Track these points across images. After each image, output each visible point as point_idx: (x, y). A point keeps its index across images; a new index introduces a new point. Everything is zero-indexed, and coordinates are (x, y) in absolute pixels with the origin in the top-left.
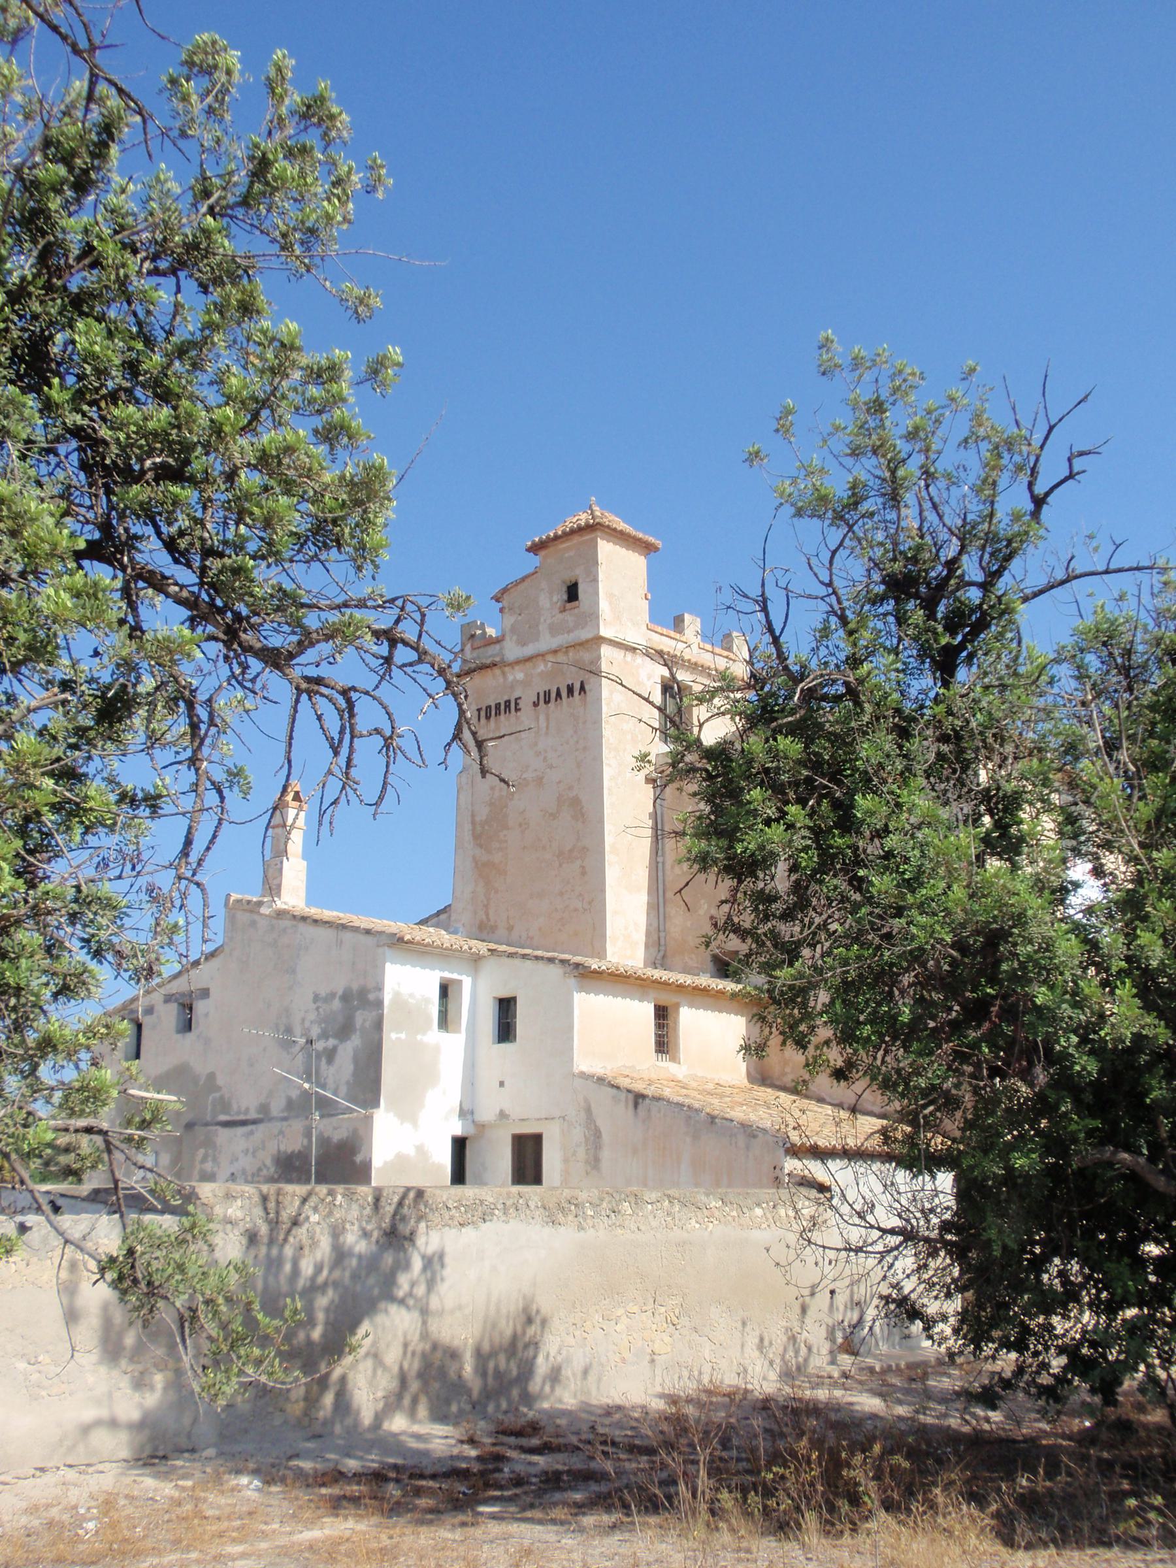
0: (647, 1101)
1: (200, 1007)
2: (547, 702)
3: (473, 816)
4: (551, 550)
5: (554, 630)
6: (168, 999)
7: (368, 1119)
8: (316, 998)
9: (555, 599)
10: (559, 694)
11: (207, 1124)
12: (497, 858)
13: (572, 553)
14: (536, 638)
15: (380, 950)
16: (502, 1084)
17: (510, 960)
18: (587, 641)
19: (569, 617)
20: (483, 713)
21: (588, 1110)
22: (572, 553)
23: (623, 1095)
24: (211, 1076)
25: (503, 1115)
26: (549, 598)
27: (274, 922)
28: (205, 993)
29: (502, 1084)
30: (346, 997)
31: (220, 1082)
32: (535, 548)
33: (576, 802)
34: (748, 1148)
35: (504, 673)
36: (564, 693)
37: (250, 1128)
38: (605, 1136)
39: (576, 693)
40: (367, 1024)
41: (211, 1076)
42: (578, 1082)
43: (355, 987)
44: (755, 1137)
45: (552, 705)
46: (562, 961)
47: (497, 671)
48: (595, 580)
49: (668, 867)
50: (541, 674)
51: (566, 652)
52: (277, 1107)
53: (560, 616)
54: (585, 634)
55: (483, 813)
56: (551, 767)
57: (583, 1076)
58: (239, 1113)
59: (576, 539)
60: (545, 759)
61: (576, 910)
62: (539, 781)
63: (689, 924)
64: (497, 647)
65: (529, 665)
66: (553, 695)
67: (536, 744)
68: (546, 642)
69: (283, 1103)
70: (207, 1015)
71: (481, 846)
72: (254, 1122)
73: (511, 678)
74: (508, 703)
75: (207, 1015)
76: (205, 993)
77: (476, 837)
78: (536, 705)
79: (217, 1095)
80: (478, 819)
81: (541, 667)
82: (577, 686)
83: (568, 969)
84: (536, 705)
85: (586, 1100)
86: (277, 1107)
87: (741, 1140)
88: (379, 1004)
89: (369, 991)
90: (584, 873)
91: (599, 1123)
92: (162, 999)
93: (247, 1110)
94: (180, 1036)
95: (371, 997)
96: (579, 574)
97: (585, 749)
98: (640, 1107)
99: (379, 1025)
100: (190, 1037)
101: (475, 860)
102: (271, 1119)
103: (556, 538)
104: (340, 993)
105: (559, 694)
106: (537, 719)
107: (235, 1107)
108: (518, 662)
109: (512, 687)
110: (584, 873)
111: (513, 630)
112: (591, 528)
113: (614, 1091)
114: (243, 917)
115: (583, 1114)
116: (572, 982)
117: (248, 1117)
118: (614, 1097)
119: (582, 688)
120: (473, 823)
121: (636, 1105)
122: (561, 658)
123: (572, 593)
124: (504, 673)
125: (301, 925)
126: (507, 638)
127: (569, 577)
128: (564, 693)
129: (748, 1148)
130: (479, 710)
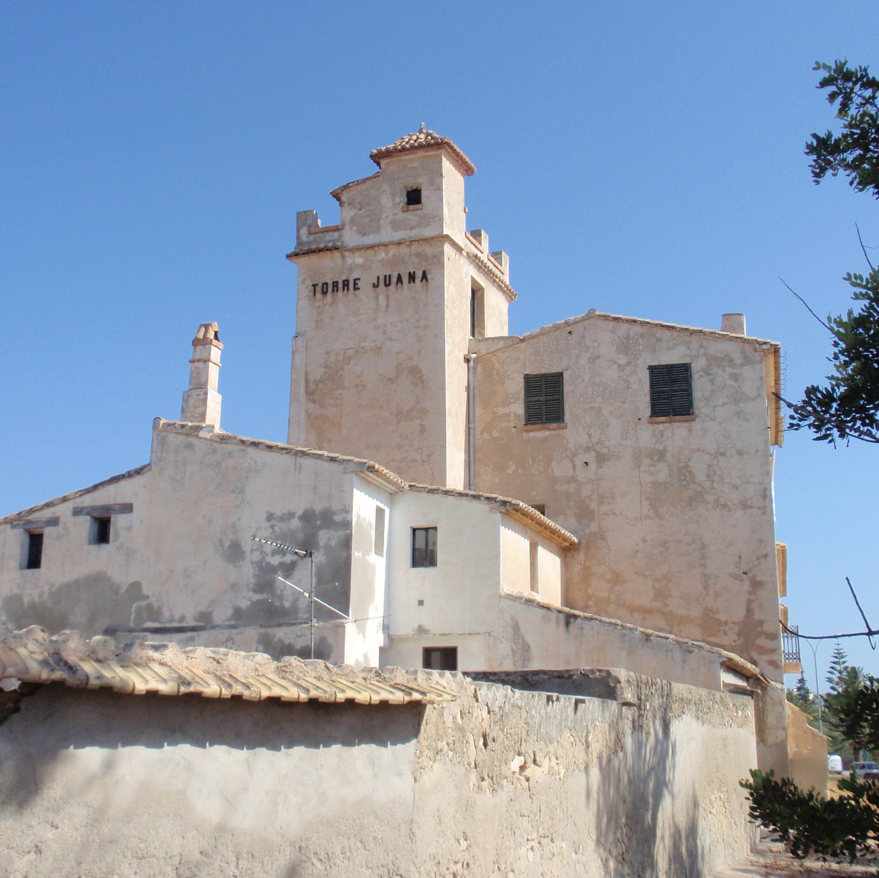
0: (579, 620)
1: (119, 522)
2: (387, 284)
3: (306, 374)
4: (394, 159)
5: (395, 225)
6: (77, 512)
7: (340, 630)
8: (270, 517)
9: (398, 200)
10: (399, 279)
11: (131, 631)
12: (332, 412)
13: (415, 165)
14: (378, 230)
15: (348, 476)
16: (421, 603)
17: (430, 496)
18: (432, 238)
19: (412, 216)
20: (319, 289)
21: (516, 628)
22: (415, 165)
23: (554, 615)
24: (136, 587)
25: (421, 630)
26: (391, 201)
27: (216, 445)
28: (127, 508)
29: (421, 603)
30: (307, 517)
31: (146, 590)
32: (377, 158)
33: (415, 371)
34: (684, 661)
35: (343, 257)
36: (405, 279)
37: (190, 634)
38: (534, 649)
39: (418, 280)
40: (333, 543)
41: (136, 587)
42: (505, 603)
43: (318, 508)
44: (690, 652)
45: (392, 288)
46: (488, 499)
47: (337, 254)
48: (440, 189)
49: (478, 433)
50: (382, 261)
51: (410, 245)
52: (221, 615)
53: (403, 215)
54: (428, 232)
55: (317, 373)
56: (390, 339)
57: (509, 597)
58: (172, 620)
59: (421, 153)
60: (384, 332)
61: (414, 461)
62: (378, 350)
63: (497, 480)
64: (336, 234)
65: (370, 252)
66: (394, 280)
67: (375, 319)
68: (387, 234)
69: (229, 612)
70: (129, 529)
71: (314, 402)
72: (193, 629)
73: (349, 261)
74: (346, 283)
75: (129, 529)
76: (127, 508)
77: (309, 393)
78: (375, 286)
79: (144, 603)
80: (311, 378)
81: (382, 255)
82: (419, 275)
83: (495, 505)
84: (375, 286)
85: (513, 618)
86: (221, 615)
87: (678, 654)
88: (347, 524)
89: (334, 513)
90: (423, 430)
91: (529, 639)
92: (70, 512)
93: (183, 618)
94: (94, 548)
95: (338, 518)
96: (422, 182)
97: (425, 327)
98: (572, 626)
99: (347, 543)
100: (105, 549)
101: (308, 415)
102: (214, 627)
103: (404, 149)
104: (300, 512)
105: (399, 279)
106: (377, 299)
107: (167, 614)
108: (359, 249)
109: (351, 269)
110: (423, 430)
111: (353, 221)
112: (439, 145)
113: (544, 611)
114: (174, 440)
115: (510, 631)
116: (498, 516)
117: (184, 624)
118: (543, 617)
119: (424, 277)
120: (307, 381)
121: (567, 624)
122: (404, 250)
123: (414, 197)
124: (343, 257)
125: (251, 451)
126: (347, 227)
127: (412, 183)
128: (405, 279)
129: (684, 661)
130: (315, 286)
